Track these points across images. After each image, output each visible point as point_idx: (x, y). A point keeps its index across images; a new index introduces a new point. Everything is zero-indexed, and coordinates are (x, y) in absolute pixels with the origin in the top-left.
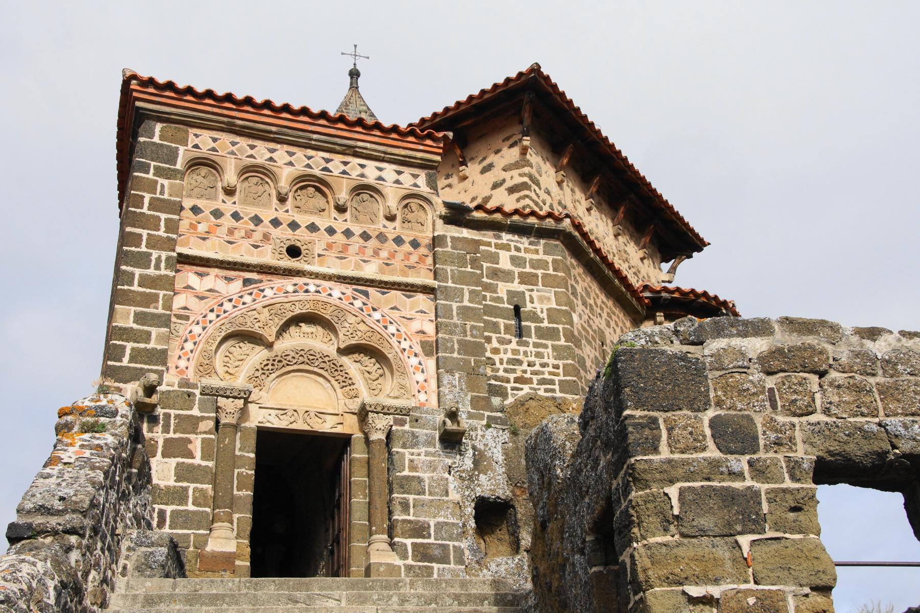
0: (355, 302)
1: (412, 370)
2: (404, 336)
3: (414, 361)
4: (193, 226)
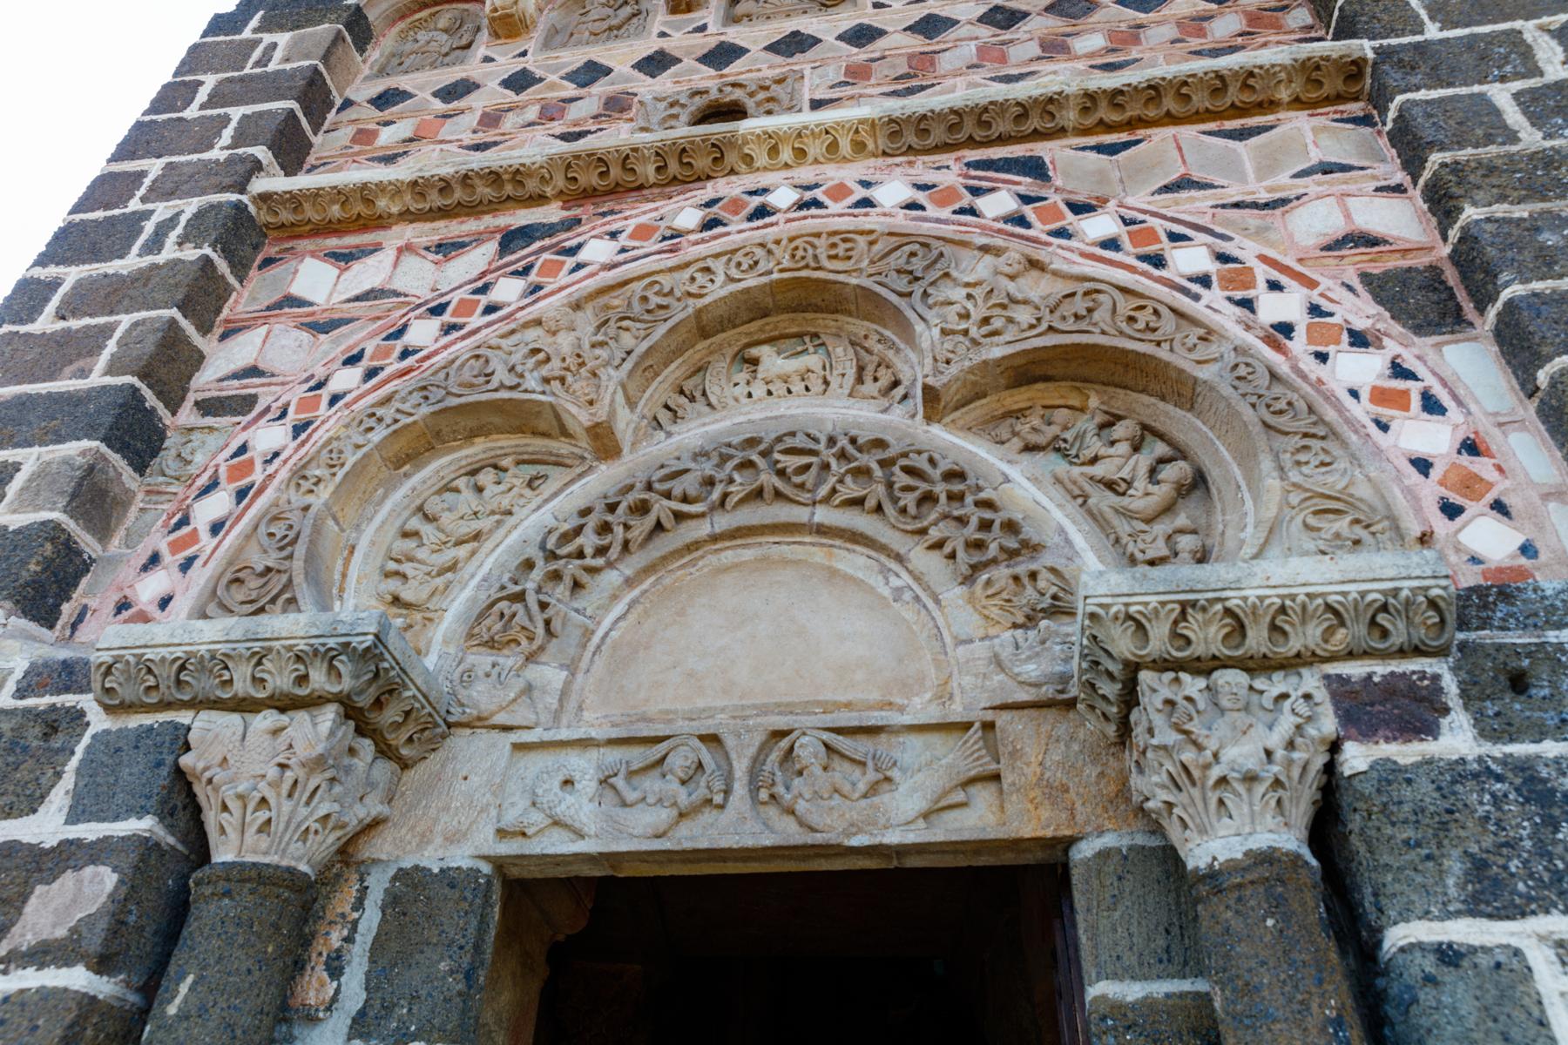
0: (981, 203)
1: (1361, 411)
2: (1262, 273)
3: (1358, 369)
4: (364, 136)
